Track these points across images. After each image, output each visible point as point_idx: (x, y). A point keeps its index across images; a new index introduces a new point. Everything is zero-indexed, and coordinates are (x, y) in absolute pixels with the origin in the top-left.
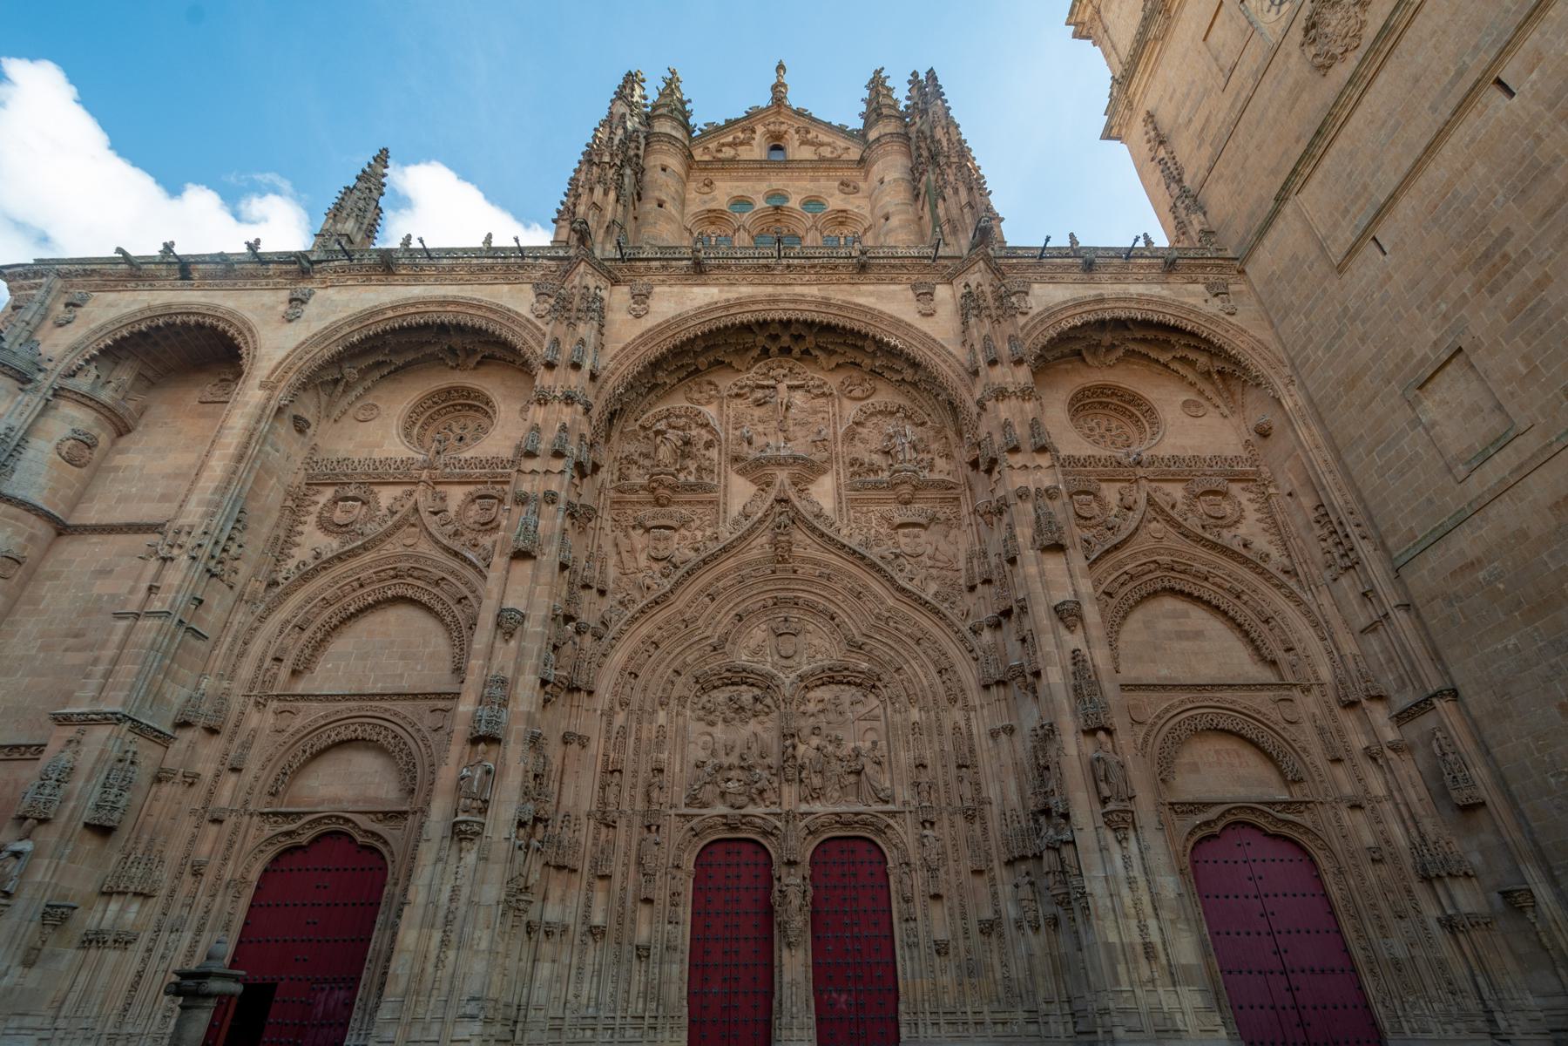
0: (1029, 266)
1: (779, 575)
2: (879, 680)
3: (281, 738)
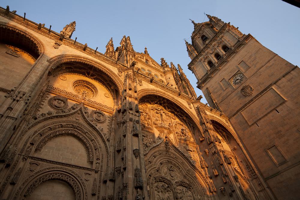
0: (203, 106)
1: (167, 155)
2: (191, 187)
3: (32, 174)
